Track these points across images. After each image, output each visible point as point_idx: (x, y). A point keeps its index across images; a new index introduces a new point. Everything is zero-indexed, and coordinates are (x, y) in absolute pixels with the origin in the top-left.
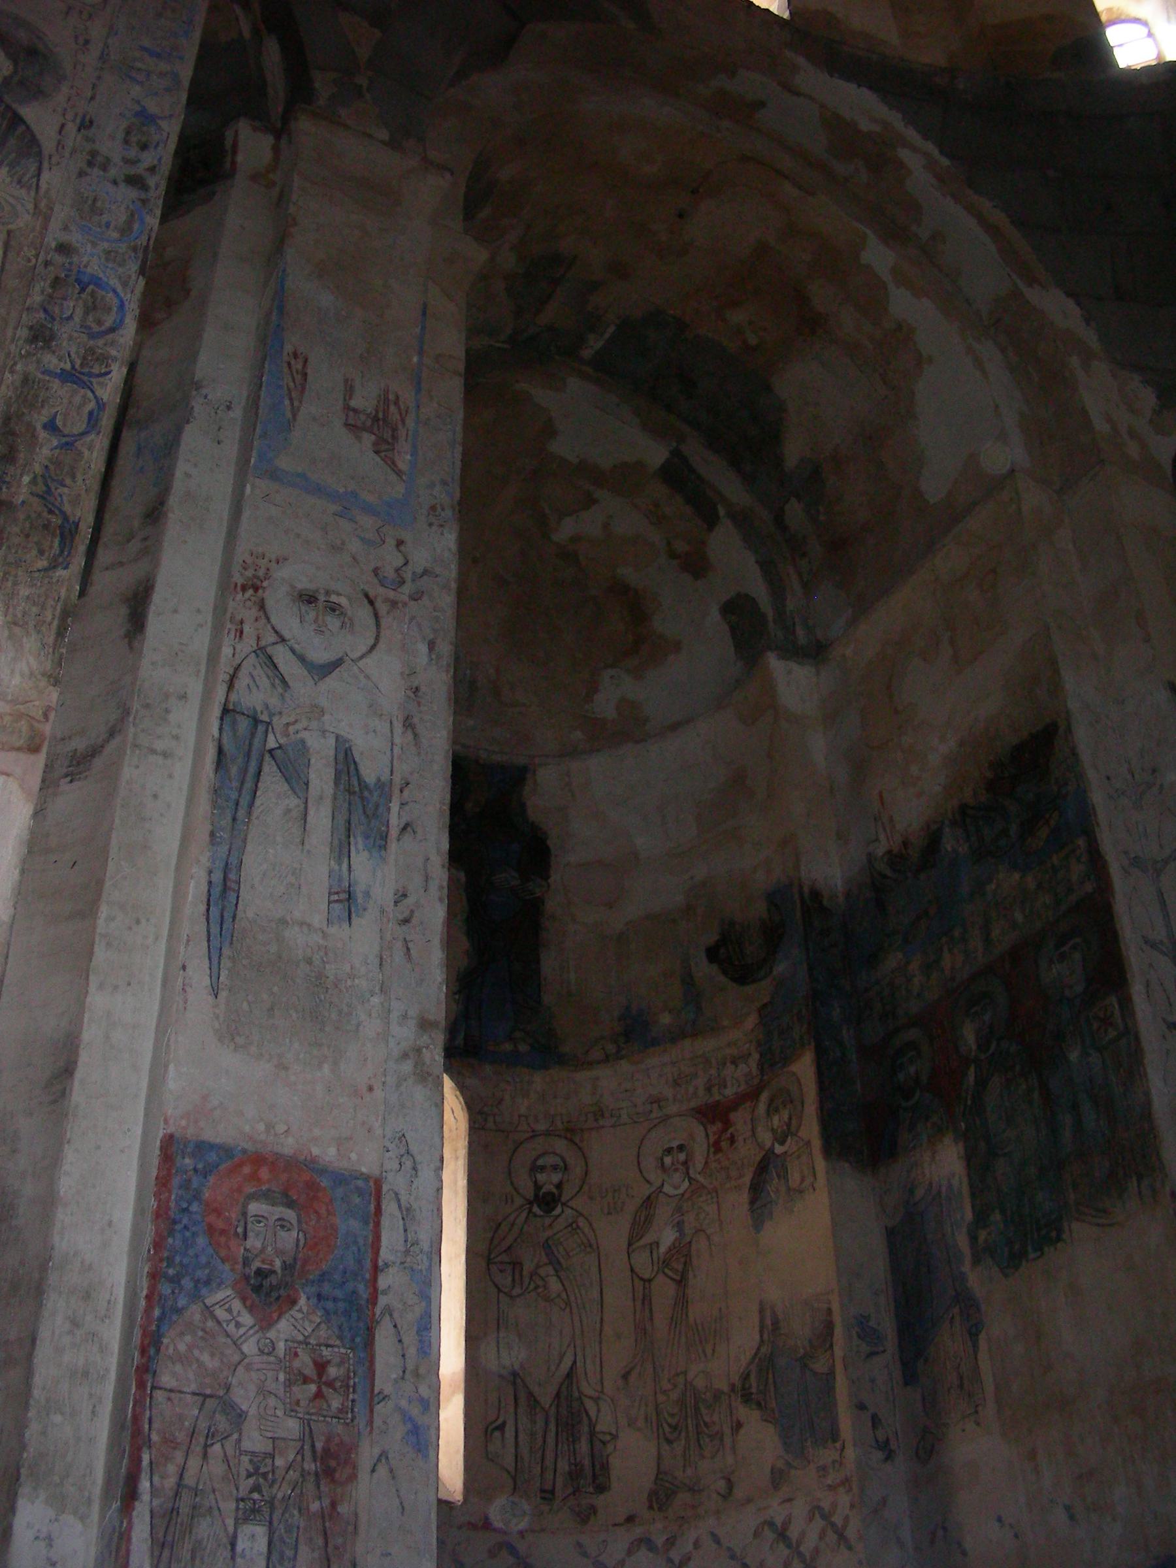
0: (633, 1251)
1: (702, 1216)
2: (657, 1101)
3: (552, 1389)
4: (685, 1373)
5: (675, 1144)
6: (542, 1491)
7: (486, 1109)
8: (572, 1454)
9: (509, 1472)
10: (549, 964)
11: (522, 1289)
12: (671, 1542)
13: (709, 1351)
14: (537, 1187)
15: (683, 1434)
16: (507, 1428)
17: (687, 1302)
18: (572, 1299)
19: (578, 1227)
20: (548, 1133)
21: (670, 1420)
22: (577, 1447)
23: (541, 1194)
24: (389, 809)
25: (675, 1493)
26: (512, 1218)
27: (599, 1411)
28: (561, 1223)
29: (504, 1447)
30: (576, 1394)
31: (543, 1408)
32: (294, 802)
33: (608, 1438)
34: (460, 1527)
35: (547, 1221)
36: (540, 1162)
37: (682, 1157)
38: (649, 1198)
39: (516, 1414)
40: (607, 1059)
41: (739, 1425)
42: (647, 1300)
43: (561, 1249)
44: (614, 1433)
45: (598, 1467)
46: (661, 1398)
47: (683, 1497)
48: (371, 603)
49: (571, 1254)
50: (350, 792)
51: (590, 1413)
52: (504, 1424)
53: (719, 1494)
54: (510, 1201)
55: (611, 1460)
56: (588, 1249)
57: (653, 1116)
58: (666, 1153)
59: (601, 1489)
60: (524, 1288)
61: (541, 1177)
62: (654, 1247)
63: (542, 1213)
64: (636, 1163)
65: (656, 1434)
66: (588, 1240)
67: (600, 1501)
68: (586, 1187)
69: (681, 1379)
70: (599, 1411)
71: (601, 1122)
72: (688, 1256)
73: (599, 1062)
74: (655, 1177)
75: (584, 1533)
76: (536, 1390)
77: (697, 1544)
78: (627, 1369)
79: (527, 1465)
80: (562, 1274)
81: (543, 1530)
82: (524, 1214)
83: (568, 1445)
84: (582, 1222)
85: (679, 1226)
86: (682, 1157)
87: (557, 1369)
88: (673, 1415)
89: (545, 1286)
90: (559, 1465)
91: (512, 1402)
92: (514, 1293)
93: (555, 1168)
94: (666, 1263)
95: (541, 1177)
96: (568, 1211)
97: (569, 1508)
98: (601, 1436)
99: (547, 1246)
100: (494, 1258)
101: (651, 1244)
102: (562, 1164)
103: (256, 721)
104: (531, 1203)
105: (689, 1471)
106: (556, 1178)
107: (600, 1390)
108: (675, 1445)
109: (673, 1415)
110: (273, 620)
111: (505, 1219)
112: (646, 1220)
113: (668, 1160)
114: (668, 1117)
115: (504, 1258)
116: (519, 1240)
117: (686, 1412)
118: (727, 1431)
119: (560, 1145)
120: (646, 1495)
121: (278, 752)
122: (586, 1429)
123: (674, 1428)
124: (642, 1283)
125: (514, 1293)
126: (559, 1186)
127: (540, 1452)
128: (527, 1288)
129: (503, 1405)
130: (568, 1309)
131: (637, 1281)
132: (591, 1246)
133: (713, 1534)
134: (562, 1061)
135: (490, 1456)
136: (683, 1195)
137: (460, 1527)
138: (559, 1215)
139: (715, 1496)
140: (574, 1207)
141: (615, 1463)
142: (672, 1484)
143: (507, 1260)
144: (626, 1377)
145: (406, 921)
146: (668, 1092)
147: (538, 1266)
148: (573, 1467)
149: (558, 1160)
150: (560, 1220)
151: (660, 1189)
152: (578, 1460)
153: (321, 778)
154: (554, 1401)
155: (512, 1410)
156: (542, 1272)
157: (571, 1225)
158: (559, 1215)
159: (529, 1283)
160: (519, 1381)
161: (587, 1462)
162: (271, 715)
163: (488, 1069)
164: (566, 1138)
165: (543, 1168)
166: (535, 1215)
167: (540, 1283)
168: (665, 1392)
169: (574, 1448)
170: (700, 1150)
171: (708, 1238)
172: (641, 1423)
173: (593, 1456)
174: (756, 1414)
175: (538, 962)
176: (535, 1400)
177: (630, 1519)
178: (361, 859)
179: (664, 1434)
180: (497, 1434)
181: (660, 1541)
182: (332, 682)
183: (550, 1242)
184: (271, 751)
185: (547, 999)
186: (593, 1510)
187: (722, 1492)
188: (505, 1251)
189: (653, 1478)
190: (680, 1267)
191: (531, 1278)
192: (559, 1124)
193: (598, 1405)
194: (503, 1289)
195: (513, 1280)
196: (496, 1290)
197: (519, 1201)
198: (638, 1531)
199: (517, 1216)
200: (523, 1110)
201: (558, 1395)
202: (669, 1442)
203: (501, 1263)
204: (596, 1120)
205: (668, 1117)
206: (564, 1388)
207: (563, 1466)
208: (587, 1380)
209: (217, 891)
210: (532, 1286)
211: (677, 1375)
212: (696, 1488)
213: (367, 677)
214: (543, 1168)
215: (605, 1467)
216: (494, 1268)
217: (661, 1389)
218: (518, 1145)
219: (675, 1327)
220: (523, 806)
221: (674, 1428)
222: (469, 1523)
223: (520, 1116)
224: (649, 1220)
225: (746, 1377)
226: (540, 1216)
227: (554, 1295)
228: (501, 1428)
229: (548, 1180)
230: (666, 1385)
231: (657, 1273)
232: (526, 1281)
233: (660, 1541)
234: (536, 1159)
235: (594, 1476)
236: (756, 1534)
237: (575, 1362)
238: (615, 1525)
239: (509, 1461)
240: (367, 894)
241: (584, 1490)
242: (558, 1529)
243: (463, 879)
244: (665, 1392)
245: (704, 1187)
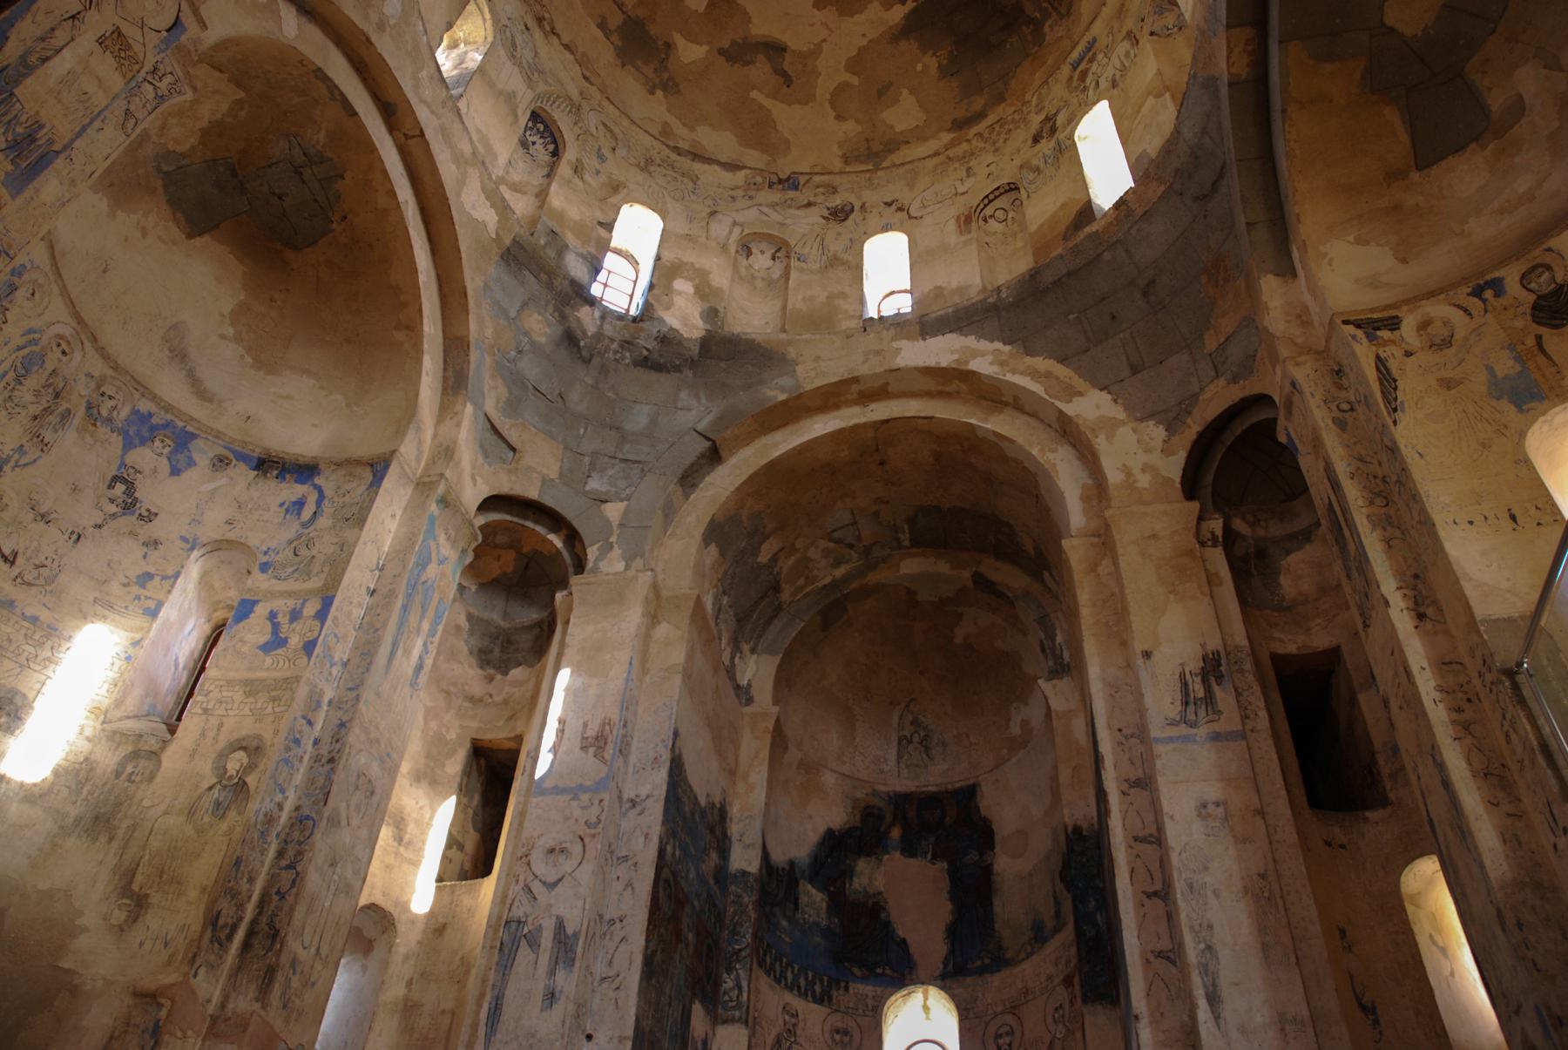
5: (1058, 1005)
10: (997, 902)
20: (1003, 1012)
24: (577, 944)
32: (534, 956)
36: (1000, 1032)
37: (1061, 1012)
40: (1028, 956)
48: (582, 840)
50: (560, 942)
71: (1028, 998)
73: (1023, 960)
74: (1052, 1028)
86: (1061, 1012)
93: (1007, 1034)
95: (1001, 1041)
103: (519, 922)
106: (1008, 1040)
110: (533, 868)
113: (1056, 1015)
119: (1009, 1018)
121: (528, 936)
145: (618, 988)
153: (547, 940)
162: (527, 917)
163: (969, 980)
165: (1001, 1036)
170: (1067, 1006)
175: (991, 904)
178: (561, 975)
182: (558, 889)
184: (525, 936)
185: (997, 926)
200: (989, 1001)
205: (1055, 987)
209: (492, 1010)
213: (575, 880)
214: (1001, 1036)
218: (987, 1024)
220: (978, 808)
240: (561, 991)
243: (946, 867)
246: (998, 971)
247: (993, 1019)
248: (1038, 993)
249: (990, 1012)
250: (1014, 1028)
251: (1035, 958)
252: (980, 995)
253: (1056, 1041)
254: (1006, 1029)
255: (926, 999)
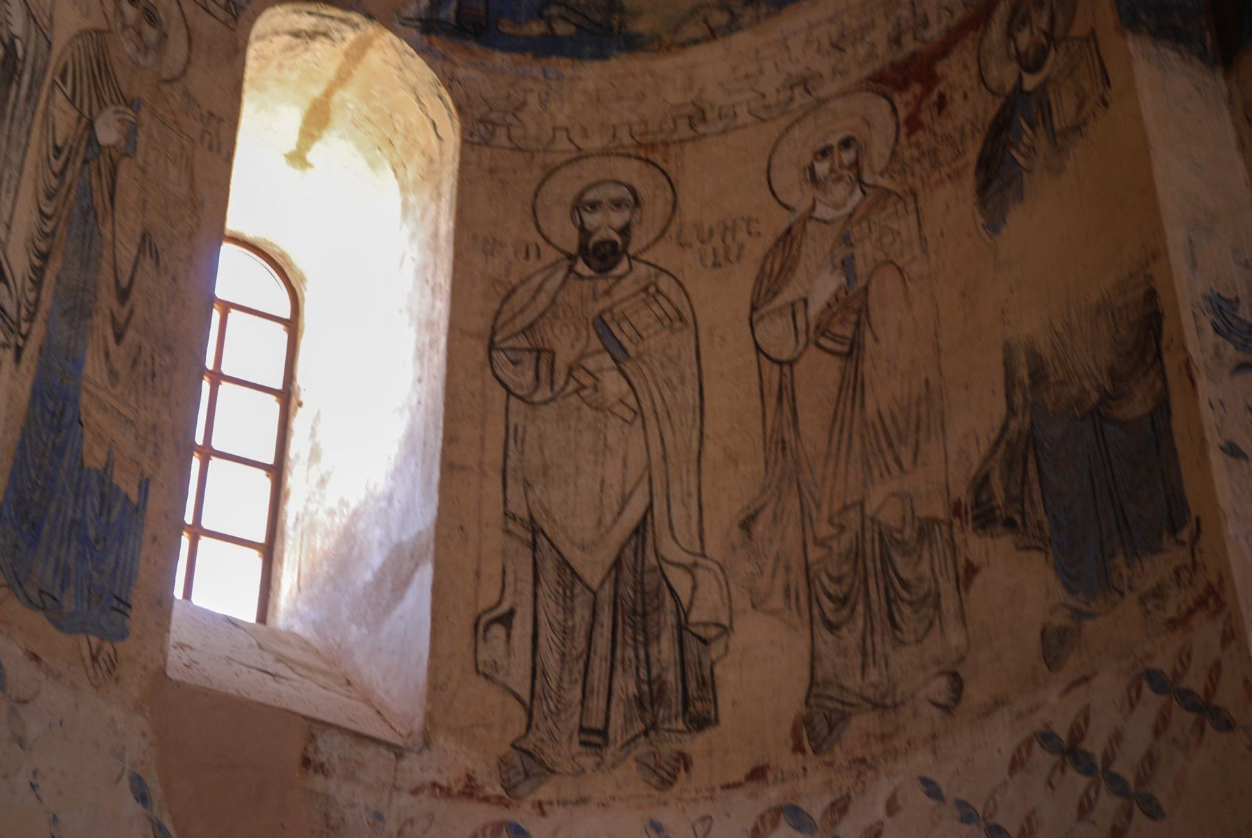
0: (762, 318)
1: (888, 239)
2: (805, 82)
3: (606, 556)
4: (862, 504)
6: (582, 730)
7: (493, 116)
8: (643, 664)
9: (518, 698)
11: (552, 389)
12: (840, 808)
13: (907, 461)
14: (584, 232)
15: (860, 608)
16: (517, 622)
17: (863, 386)
18: (646, 404)
19: (658, 291)
20: (605, 153)
21: (832, 588)
22: (653, 650)
23: (591, 245)
25: (845, 717)
26: (537, 280)
27: (694, 588)
28: (627, 287)
29: (509, 653)
30: (651, 559)
31: (589, 589)
33: (713, 632)
34: (415, 792)
35: (602, 285)
36: (591, 196)
37: (848, 156)
38: (789, 231)
39: (535, 596)
40: (713, 34)
41: (972, 570)
42: (786, 394)
43: (625, 326)
44: (725, 622)
45: (692, 685)
46: (814, 553)
47: (863, 722)
49: (644, 334)
51: (679, 592)
52: (511, 613)
53: (936, 704)
54: (533, 253)
55: (718, 670)
56: (678, 324)
57: (795, 105)
58: (820, 157)
59: (701, 723)
60: (557, 388)
61: (592, 219)
62: (800, 306)
63: (592, 273)
64: (764, 181)
65: (806, 617)
66: (678, 311)
67: (695, 745)
68: (673, 229)
69: (854, 515)
70: (694, 588)
72: (863, 313)
74: (800, 198)
75: (665, 804)
76: (576, 558)
77: (892, 807)
78: (751, 511)
79: (553, 685)
80: (629, 367)
81: (583, 801)
82: (560, 275)
83: (636, 649)
84: (665, 283)
85: (847, 265)
86: (848, 156)
87: (615, 521)
88: (838, 580)
89: (596, 388)
90: (618, 682)
91: (530, 578)
92: (538, 397)
93: (617, 204)
94: (822, 329)
95: (592, 219)
96: (641, 269)
97: (636, 760)
98: (700, 631)
99: (601, 326)
100: (504, 340)
101: (793, 305)
102: (631, 198)
104: (571, 257)
105: (873, 675)
106: (618, 219)
107: (698, 550)
108: (844, 631)
109: (838, 580)
111: (522, 282)
112: (781, 269)
113: (822, 168)
114: (822, 102)
115: (523, 343)
116: (549, 315)
117: (865, 569)
118: (947, 587)
119: (629, 171)
120: (787, 728)
122: (670, 620)
123: (842, 601)
124: (776, 367)
125: (538, 397)
126: (625, 231)
127: (581, 665)
128: (563, 389)
129: (510, 578)
130: (638, 422)
131: (766, 363)
132: (681, 319)
133: (926, 782)
134: (633, 44)
135: (481, 668)
136: (851, 216)
137: (415, 792)
138: (620, 278)
139: (927, 710)
140: (652, 260)
141: (727, 676)
142: (843, 703)
143: (526, 344)
144: (746, 525)
146: (823, 65)
147: (583, 355)
148: (645, 687)
149: (623, 192)
150: (625, 282)
151: (809, 216)
152: (655, 672)
154: (609, 573)
155: (527, 588)
156: (591, 364)
157: (645, 289)
158: (620, 278)
159: (567, 383)
160: (542, 541)
161: (671, 677)
164: (639, 158)
165: (594, 206)
166: (580, 277)
167: (588, 381)
168: (822, 543)
169: (647, 656)
171: (900, 270)
172: (777, 601)
173: (683, 663)
174: (1005, 542)
176: (574, 573)
177: (758, 774)
179: (823, 614)
180: (498, 631)
181: (816, 808)
183: (607, 317)
186: (684, 761)
187: (942, 699)
188: (523, 331)
189: (802, 694)
190: (848, 332)
191: (570, 374)
192: (627, 140)
193: (694, 577)
194: (519, 392)
195: (537, 377)
196: (500, 392)
197: (550, 255)
198: (773, 795)
199: (546, 279)
200: (562, 119)
201: (617, 564)
202: (832, 627)
203: (514, 349)
204: (692, 126)
205: (822, 102)
206: (629, 552)
207: (626, 685)
208: (674, 537)
210: (572, 386)
211: (846, 508)
212: (888, 701)
214: (594, 206)
215: (708, 684)
216: (500, 357)
217: (815, 538)
218: (550, 173)
219: (841, 431)
221: (842, 601)
222: (435, 785)
223: (554, 129)
224: (787, 270)
225: (981, 484)
226: (590, 278)
227: (613, 400)
228: (506, 620)
229: (605, 224)
230: (825, 530)
231: (806, 346)
232: (560, 379)
233: (816, 808)
234: (582, 194)
235: (686, 702)
236: (1016, 764)
237: (650, 507)
238: (727, 787)
239: (519, 678)
241: (667, 726)
242: (614, 798)
244: (822, 543)
245: (889, 192)
246: (601, 56)
247: (569, 163)
248: (743, 116)
249: (563, 143)
250: (644, 191)
251: (742, 40)
252: (533, 100)
253: (811, 226)
254: (616, 192)
255: (342, 79)
